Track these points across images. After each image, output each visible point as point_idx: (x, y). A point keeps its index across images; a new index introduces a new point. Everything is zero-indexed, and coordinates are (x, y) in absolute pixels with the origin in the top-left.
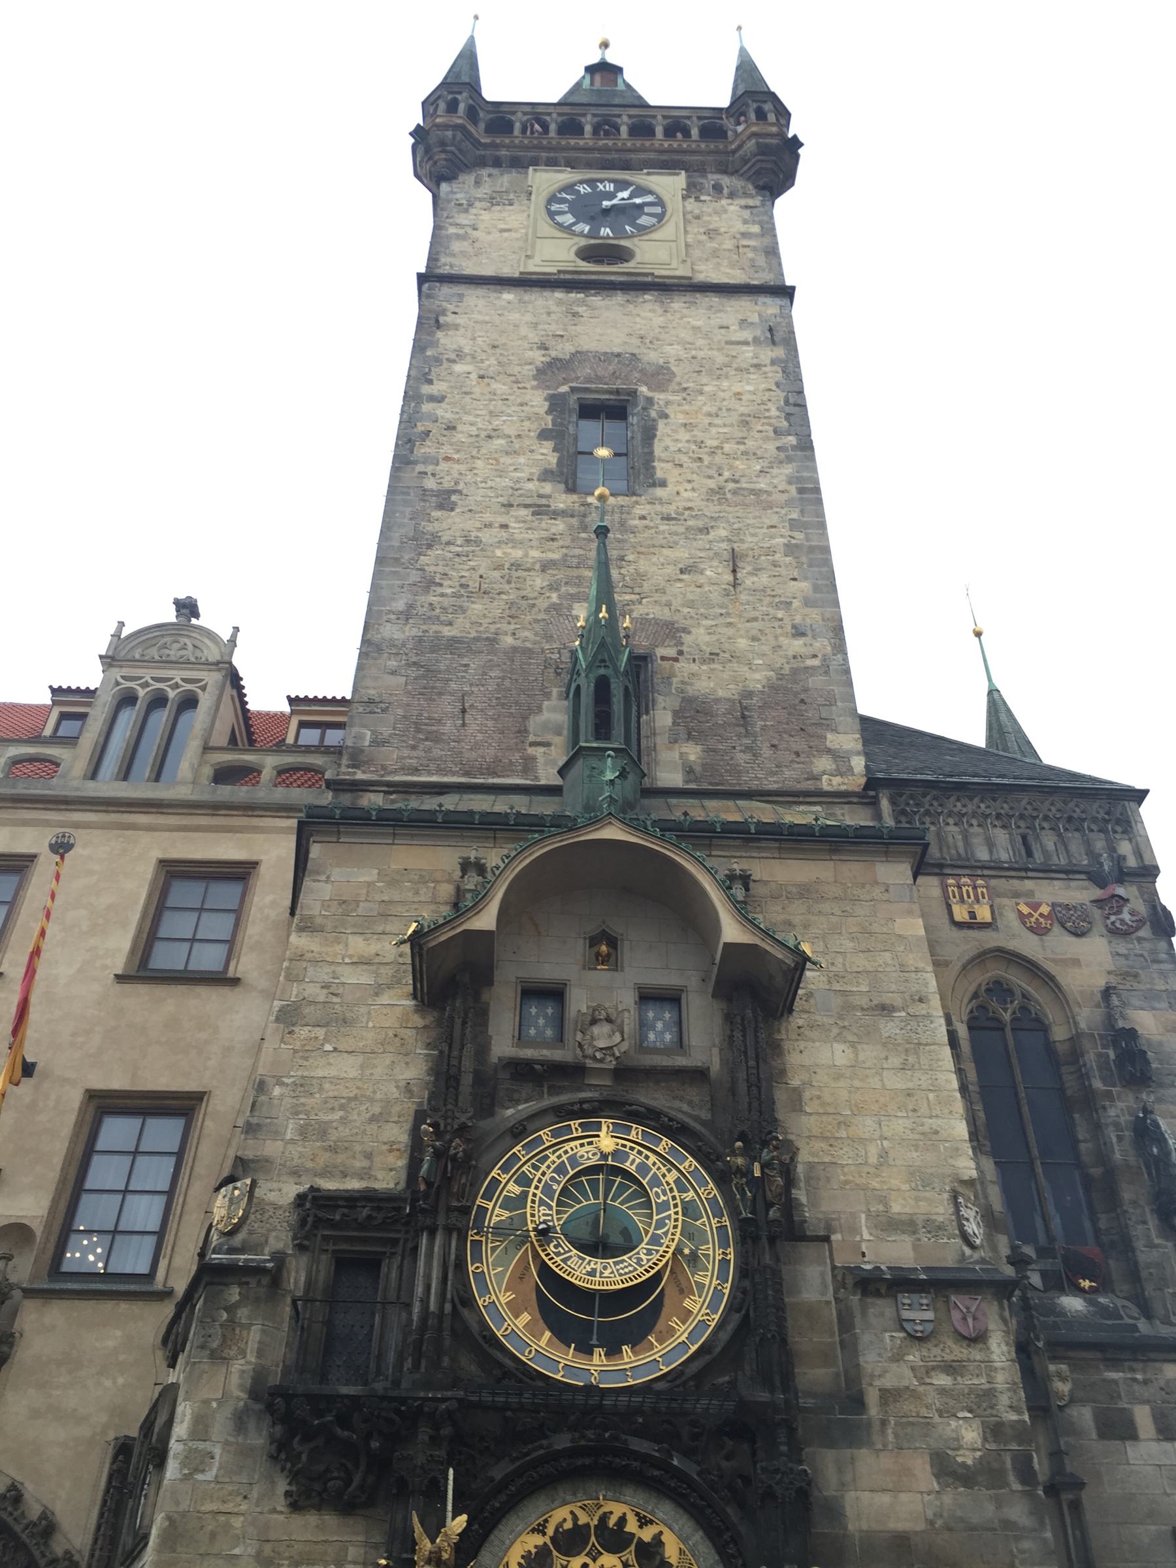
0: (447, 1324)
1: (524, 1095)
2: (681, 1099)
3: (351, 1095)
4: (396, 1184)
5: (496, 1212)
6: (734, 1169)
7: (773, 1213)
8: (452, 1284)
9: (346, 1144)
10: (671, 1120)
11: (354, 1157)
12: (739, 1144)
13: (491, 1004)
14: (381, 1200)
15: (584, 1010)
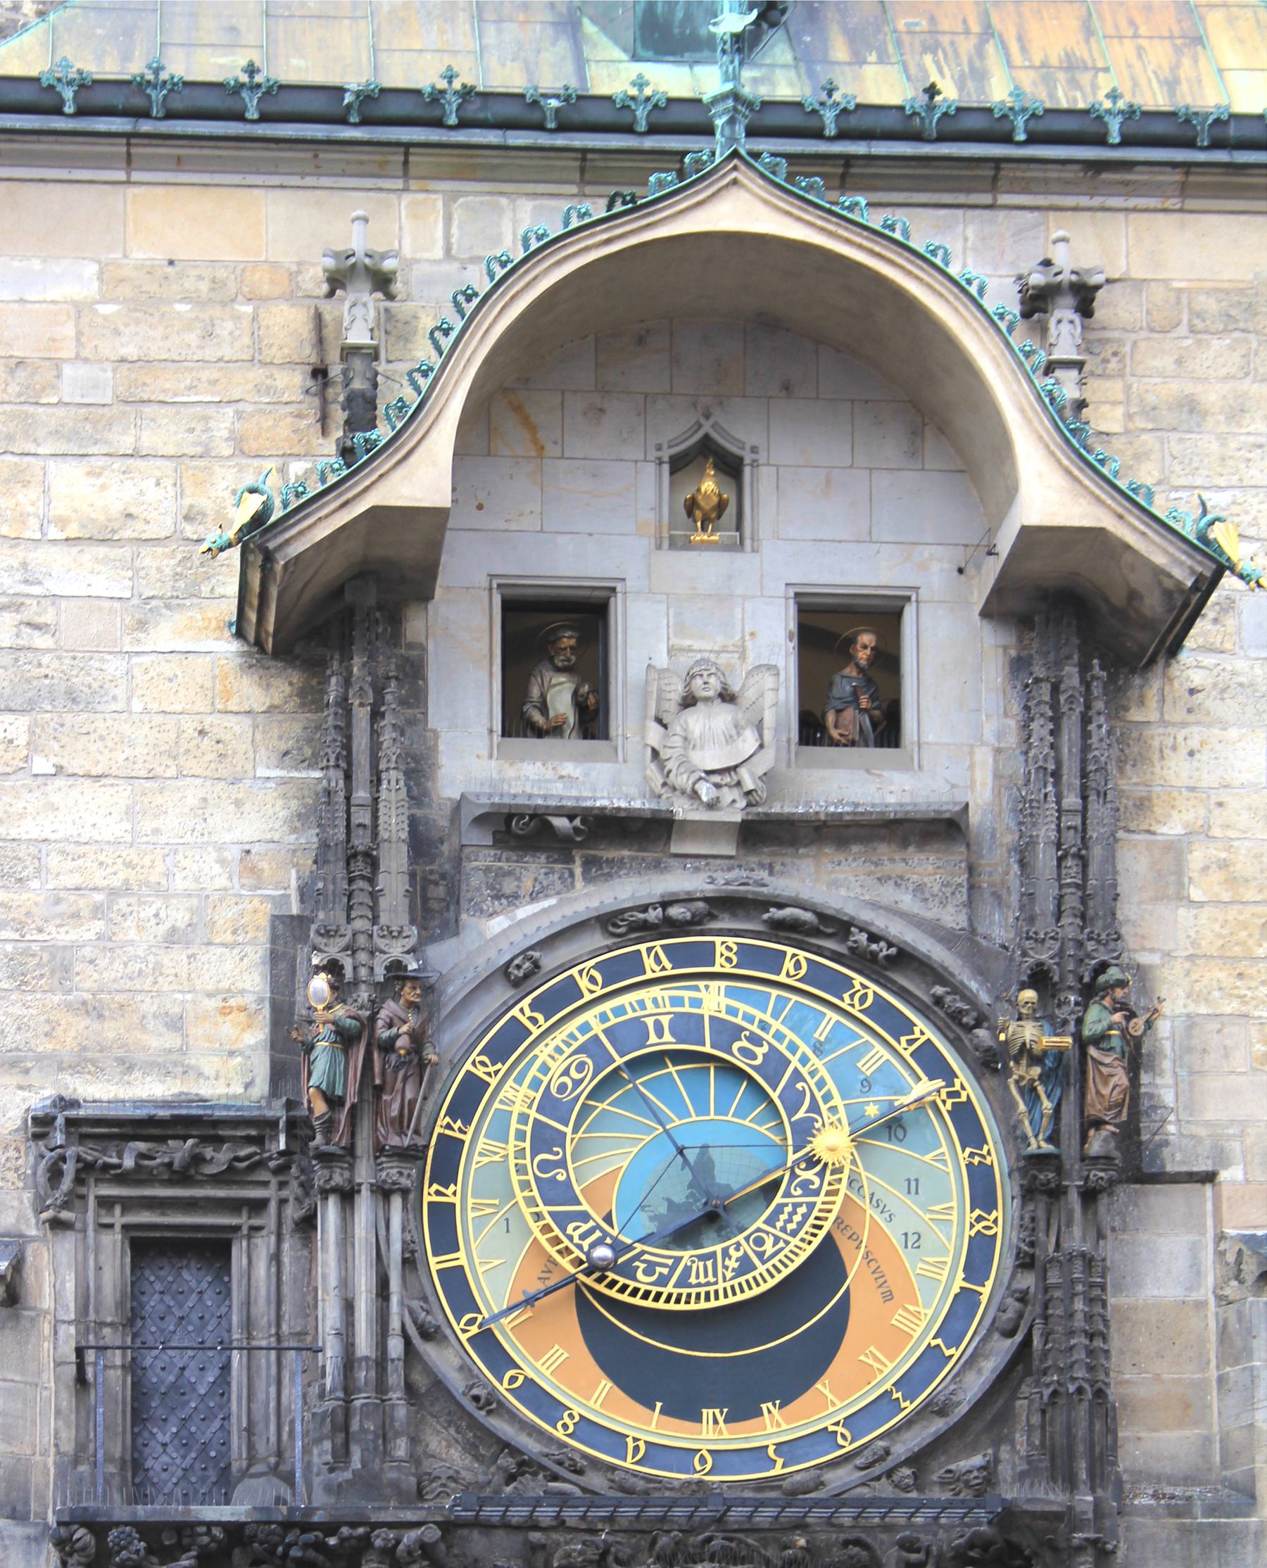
0: (395, 1377)
1: (528, 884)
2: (899, 881)
3: (116, 882)
4: (247, 1086)
5: (478, 1149)
6: (1014, 1050)
7: (1096, 1145)
8: (402, 1304)
9: (120, 998)
10: (874, 938)
11: (144, 1027)
12: (1029, 995)
13: (431, 647)
14: (217, 1123)
15: (662, 660)
